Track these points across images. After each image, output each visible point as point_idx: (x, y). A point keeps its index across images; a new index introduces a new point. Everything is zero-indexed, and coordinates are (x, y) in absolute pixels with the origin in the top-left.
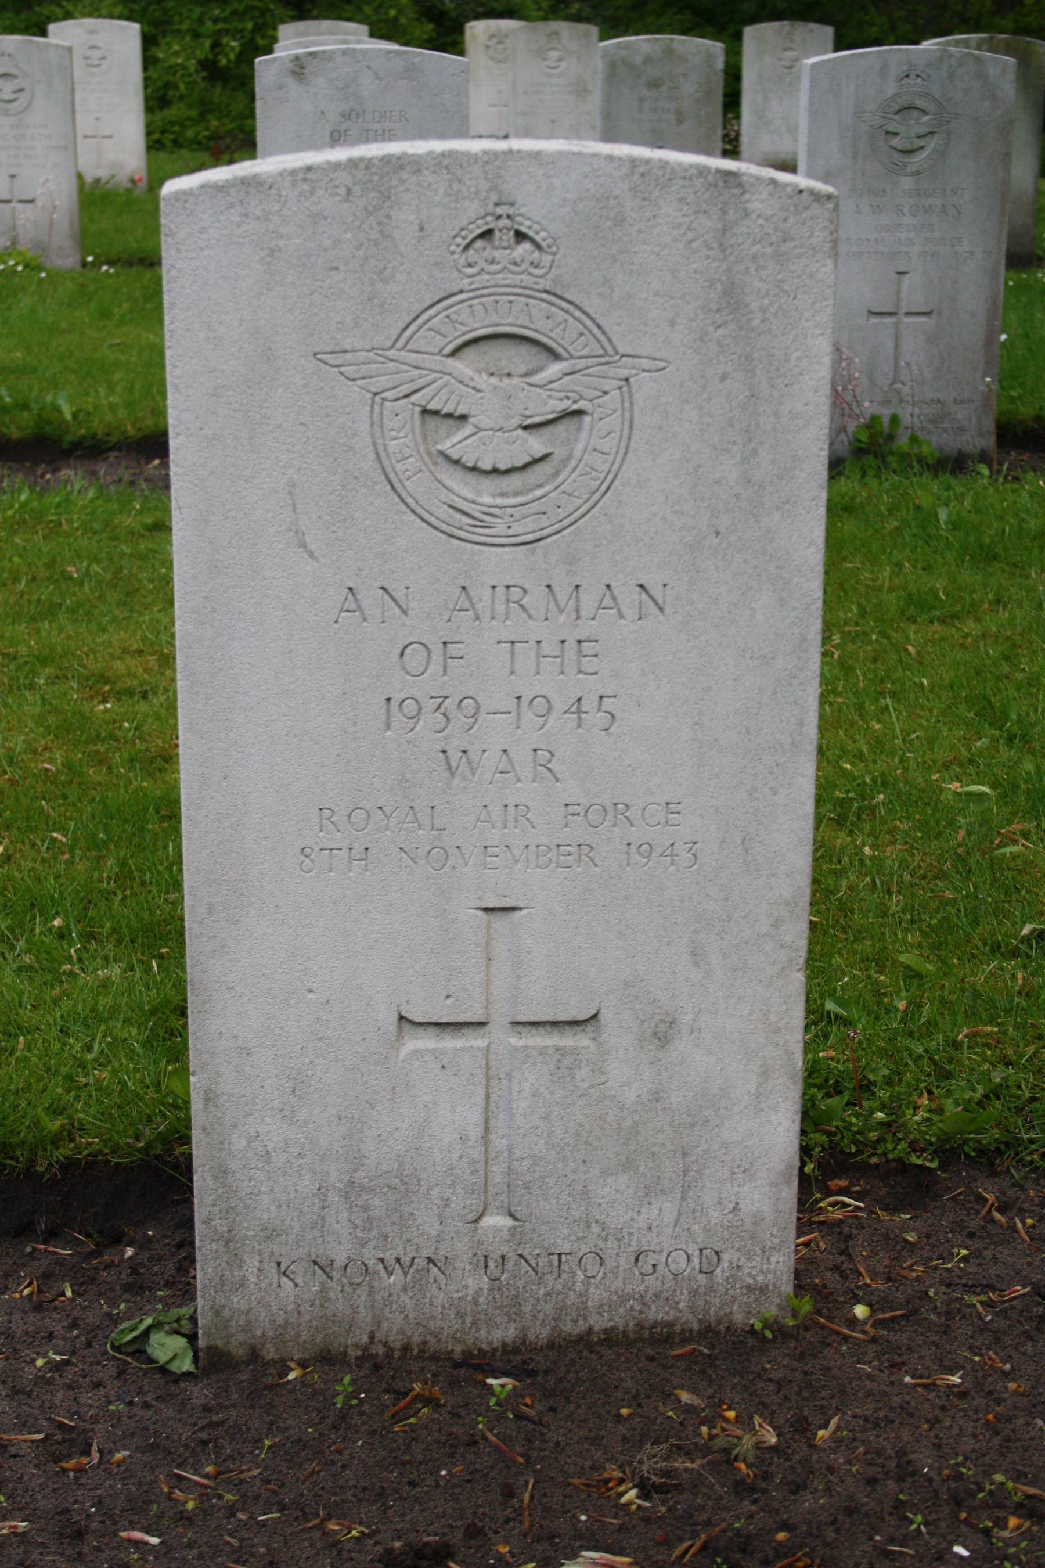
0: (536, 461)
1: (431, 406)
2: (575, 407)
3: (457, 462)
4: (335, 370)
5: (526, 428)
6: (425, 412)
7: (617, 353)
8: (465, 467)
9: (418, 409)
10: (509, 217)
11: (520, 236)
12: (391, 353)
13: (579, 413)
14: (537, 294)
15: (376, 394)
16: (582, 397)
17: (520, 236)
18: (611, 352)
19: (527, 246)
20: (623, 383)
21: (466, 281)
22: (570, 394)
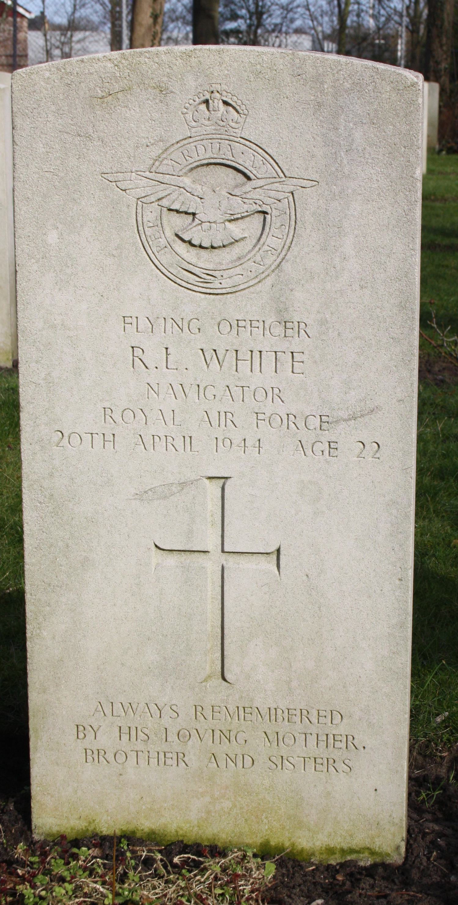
0: (237, 241)
1: (171, 208)
2: (260, 209)
3: (190, 243)
4: (114, 184)
5: (230, 221)
6: (170, 210)
7: (285, 176)
8: (194, 245)
9: (165, 209)
10: (218, 92)
11: (225, 103)
12: (147, 174)
13: (265, 213)
14: (236, 139)
15: (138, 199)
16: (263, 204)
17: (225, 103)
18: (281, 175)
19: (231, 109)
20: (290, 194)
21: (193, 130)
22: (257, 201)
